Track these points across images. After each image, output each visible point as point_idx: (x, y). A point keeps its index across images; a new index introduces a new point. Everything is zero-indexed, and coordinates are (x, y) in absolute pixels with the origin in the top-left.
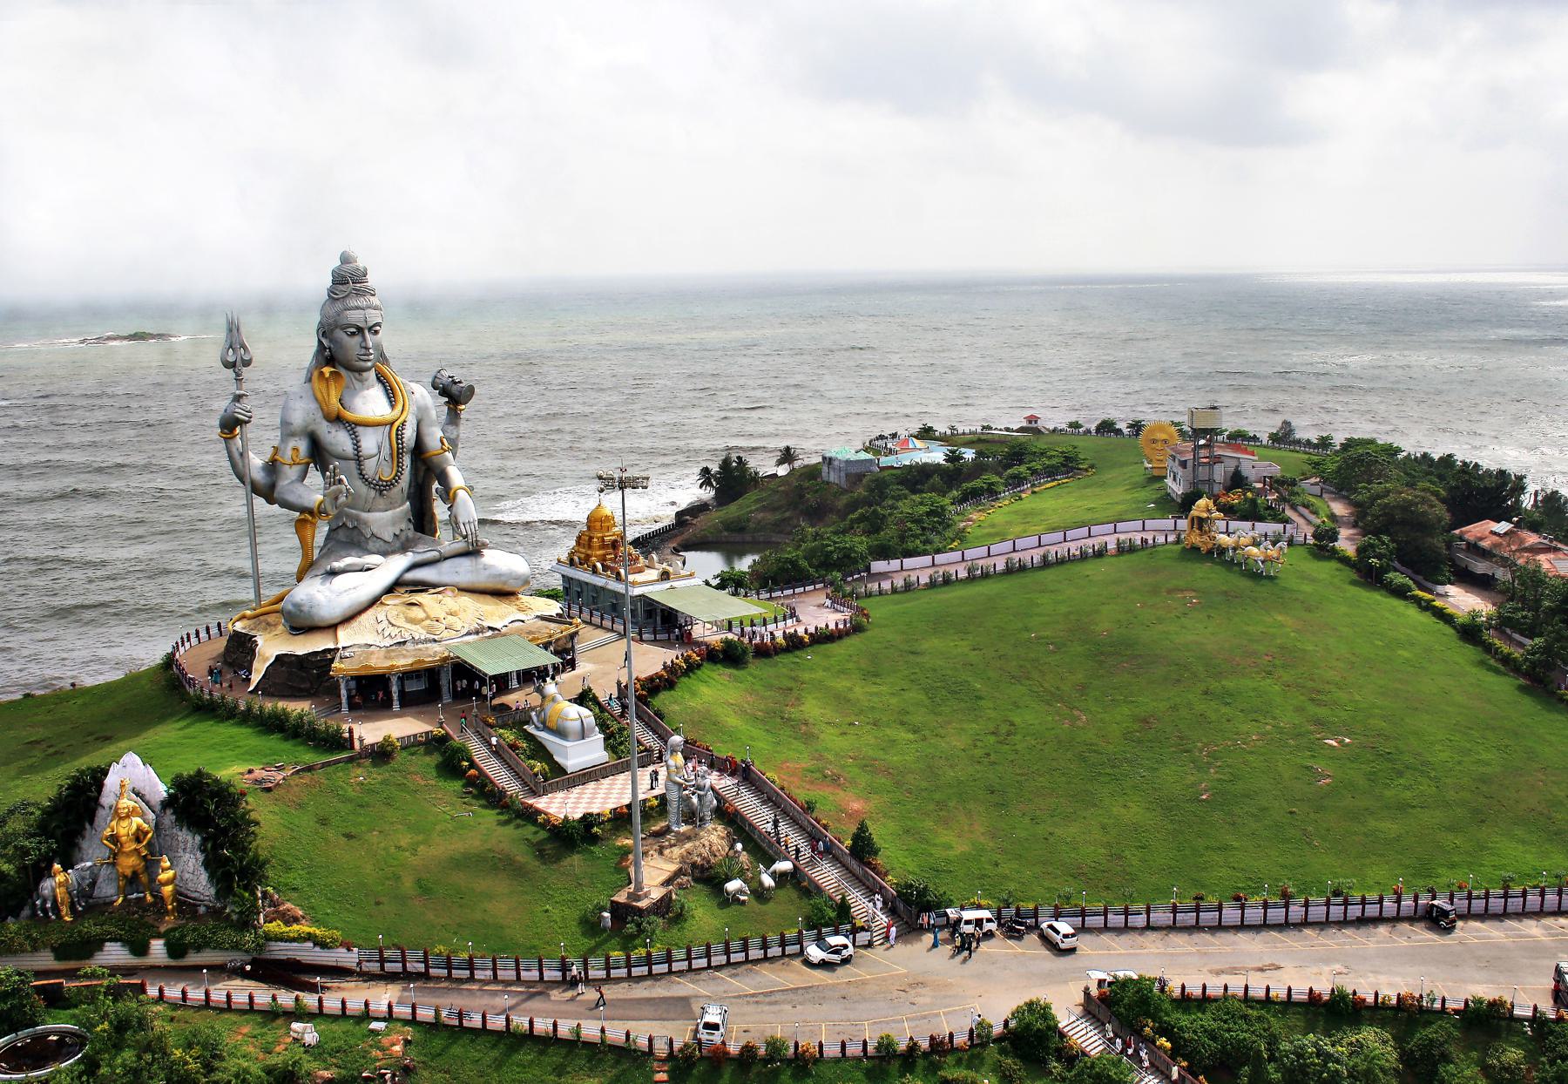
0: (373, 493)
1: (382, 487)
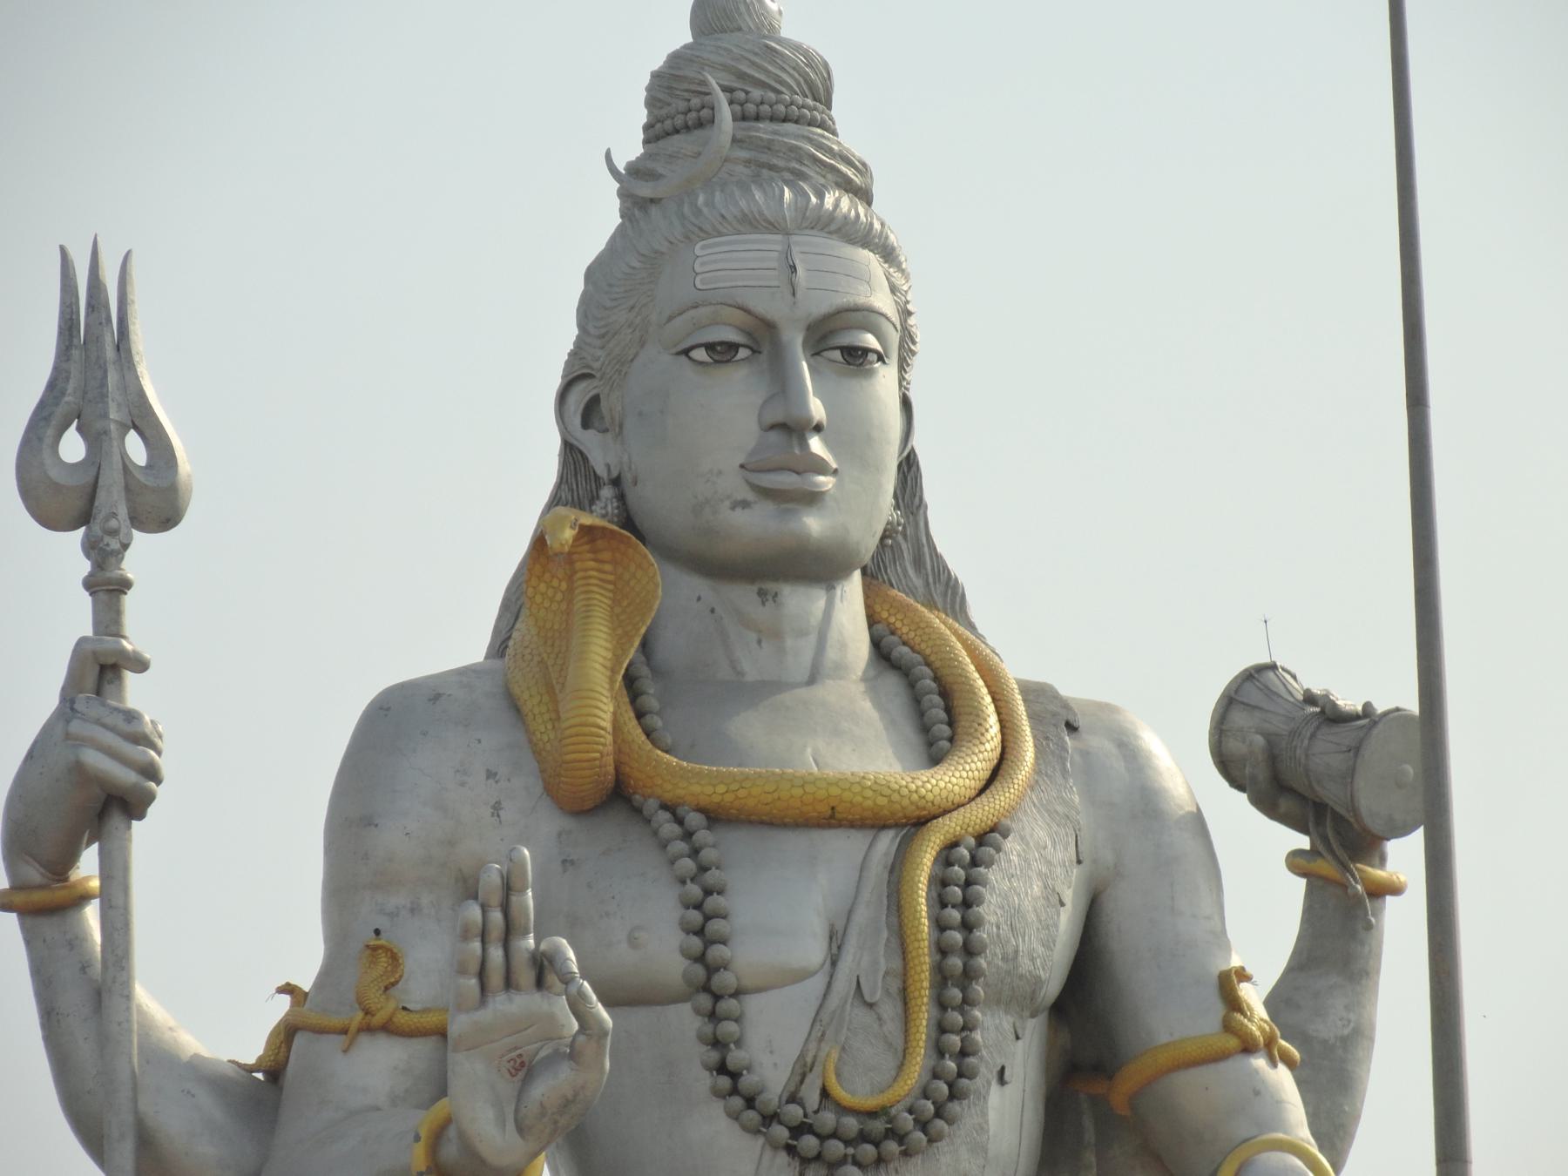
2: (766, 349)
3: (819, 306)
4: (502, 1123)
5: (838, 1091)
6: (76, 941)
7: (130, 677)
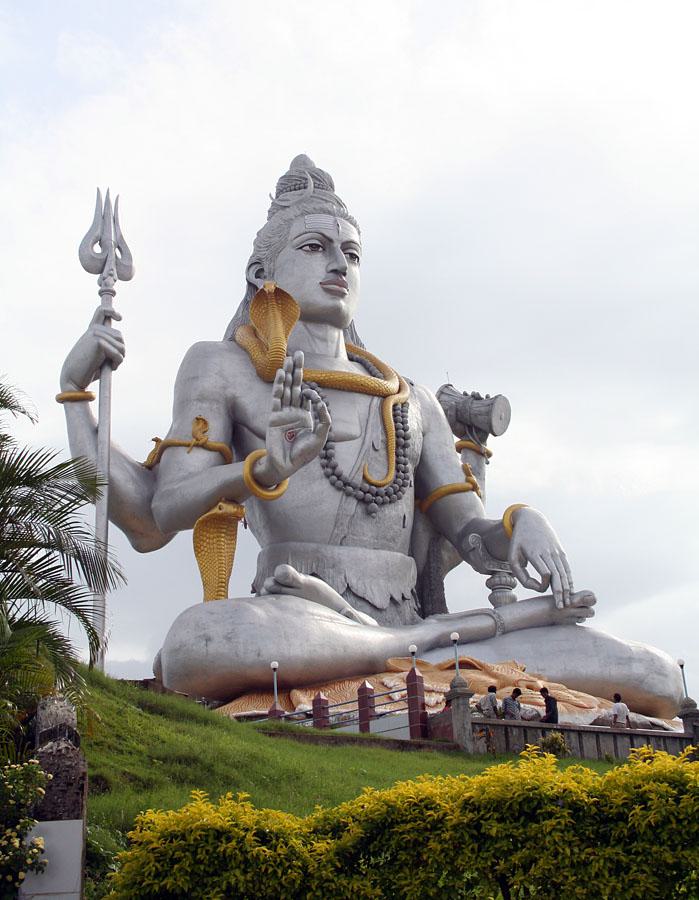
0: (352, 505)
1: (370, 498)
2: (327, 250)
3: (345, 239)
4: (285, 458)
5: (369, 477)
6: (87, 414)
7: (113, 321)
